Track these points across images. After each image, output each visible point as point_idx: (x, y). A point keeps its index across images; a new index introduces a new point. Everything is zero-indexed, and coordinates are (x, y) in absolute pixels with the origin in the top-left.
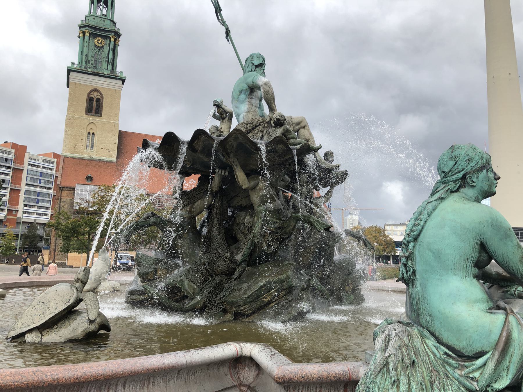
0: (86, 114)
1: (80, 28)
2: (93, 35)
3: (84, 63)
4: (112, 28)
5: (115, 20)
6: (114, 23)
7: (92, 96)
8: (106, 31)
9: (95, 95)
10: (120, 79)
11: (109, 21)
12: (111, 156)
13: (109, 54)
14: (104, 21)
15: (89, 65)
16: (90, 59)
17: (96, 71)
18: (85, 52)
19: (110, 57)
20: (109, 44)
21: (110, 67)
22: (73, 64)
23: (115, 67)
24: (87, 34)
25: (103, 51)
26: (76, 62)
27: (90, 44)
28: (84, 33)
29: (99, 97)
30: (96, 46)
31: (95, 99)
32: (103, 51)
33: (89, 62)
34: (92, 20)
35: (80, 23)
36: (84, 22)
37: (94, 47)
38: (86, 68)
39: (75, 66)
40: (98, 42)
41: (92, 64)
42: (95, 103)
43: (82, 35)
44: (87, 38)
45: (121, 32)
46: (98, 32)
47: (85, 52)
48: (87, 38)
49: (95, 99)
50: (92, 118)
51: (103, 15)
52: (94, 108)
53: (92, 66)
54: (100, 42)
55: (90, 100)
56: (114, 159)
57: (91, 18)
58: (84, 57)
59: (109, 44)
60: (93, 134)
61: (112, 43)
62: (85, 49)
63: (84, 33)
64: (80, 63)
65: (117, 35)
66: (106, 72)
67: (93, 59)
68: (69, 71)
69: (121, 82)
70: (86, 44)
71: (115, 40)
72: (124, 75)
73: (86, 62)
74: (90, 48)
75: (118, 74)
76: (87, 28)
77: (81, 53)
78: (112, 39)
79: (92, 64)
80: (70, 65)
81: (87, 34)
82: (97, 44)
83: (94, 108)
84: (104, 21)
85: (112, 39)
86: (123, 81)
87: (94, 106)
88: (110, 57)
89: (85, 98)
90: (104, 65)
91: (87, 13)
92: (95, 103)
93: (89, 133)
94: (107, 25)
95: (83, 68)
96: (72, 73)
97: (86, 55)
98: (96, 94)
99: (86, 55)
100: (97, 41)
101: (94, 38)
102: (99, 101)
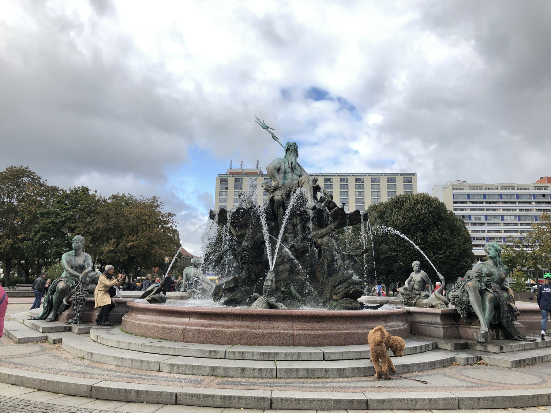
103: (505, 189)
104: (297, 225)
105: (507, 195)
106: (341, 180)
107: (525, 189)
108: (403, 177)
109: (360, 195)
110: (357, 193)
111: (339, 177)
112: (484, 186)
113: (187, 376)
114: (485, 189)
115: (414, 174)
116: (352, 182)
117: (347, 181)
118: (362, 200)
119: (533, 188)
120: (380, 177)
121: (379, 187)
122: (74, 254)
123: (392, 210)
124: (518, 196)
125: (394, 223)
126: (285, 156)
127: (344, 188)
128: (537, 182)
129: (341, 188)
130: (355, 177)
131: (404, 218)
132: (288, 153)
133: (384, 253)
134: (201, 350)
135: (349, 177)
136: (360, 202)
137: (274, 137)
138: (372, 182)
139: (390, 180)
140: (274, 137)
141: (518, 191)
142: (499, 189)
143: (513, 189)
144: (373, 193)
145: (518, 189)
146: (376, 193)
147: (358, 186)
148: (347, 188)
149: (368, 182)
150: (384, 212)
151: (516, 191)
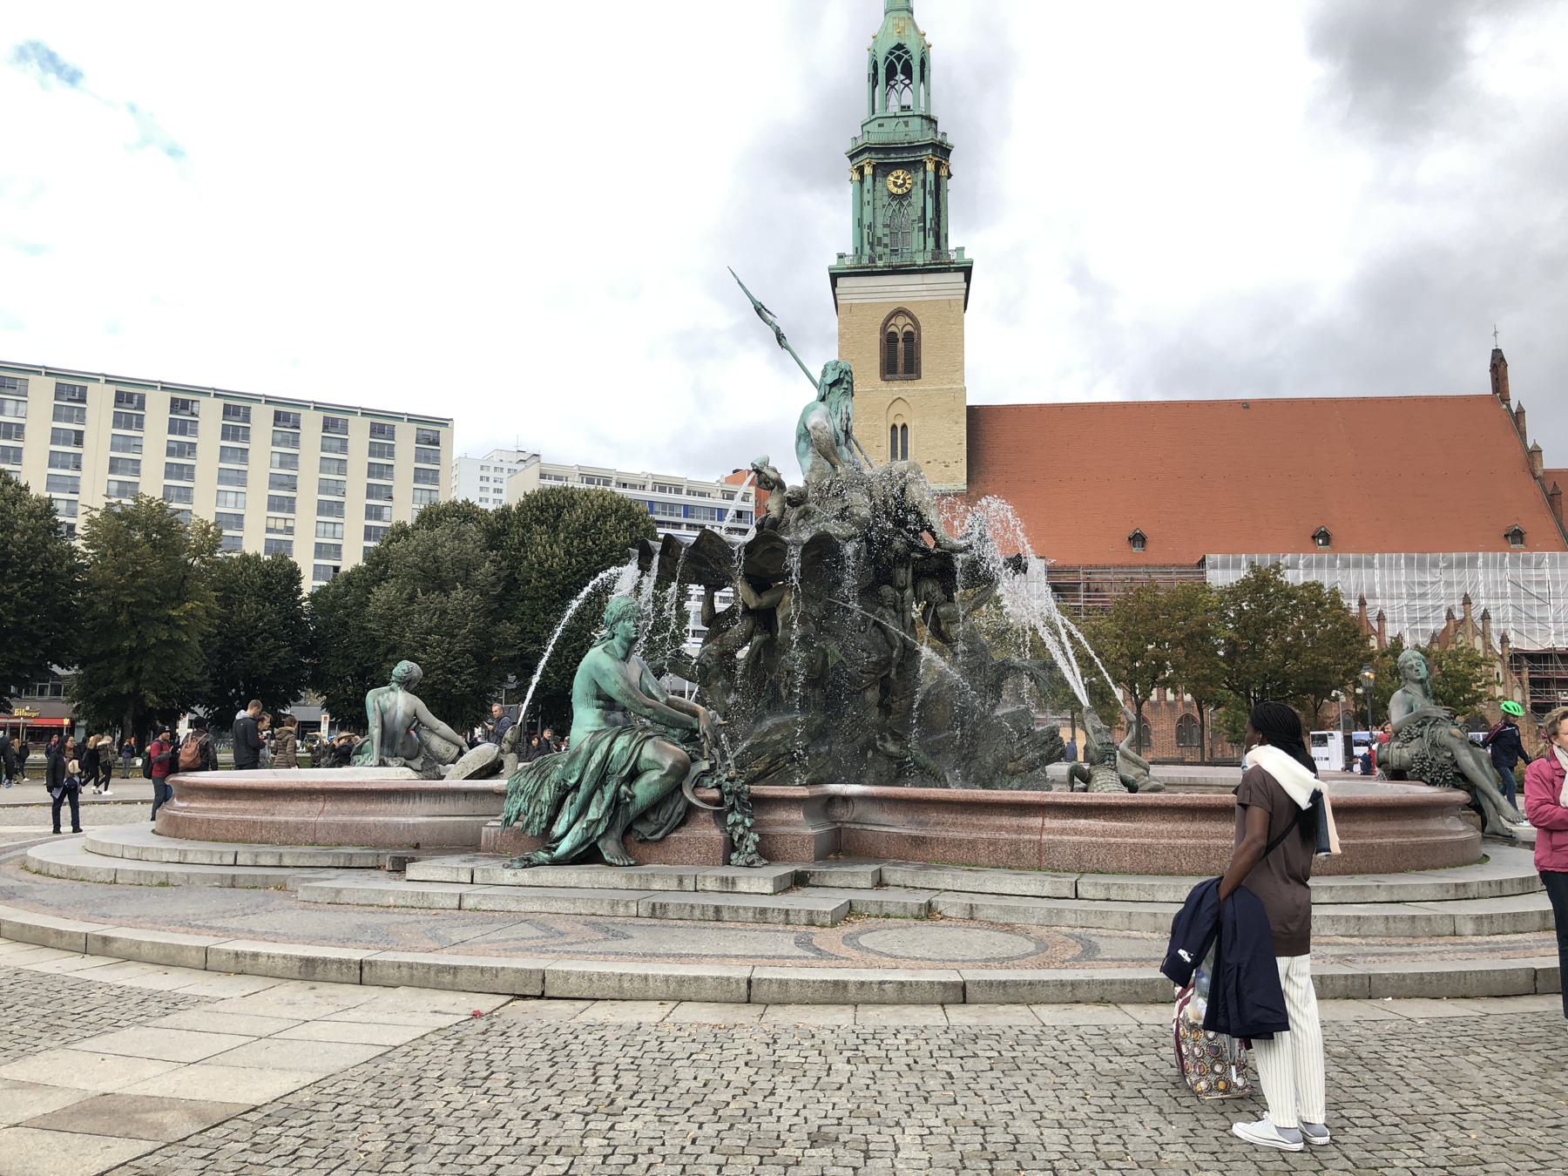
0: (883, 379)
1: (851, 158)
2: (882, 169)
3: (867, 248)
4: (929, 137)
5: (933, 114)
6: (931, 121)
7: (893, 329)
8: (912, 148)
9: (900, 326)
10: (958, 270)
11: (918, 121)
12: (953, 479)
13: (924, 209)
14: (906, 124)
15: (879, 249)
16: (879, 233)
17: (896, 261)
18: (866, 222)
19: (929, 214)
20: (924, 182)
21: (931, 242)
22: (841, 256)
23: (942, 240)
24: (868, 171)
25: (910, 204)
26: (850, 251)
27: (878, 195)
28: (861, 170)
29: (909, 328)
30: (893, 196)
31: (900, 336)
32: (910, 204)
33: (880, 239)
34: (877, 129)
35: (849, 147)
36: (860, 142)
37: (886, 200)
38: (872, 260)
39: (847, 262)
40: (895, 184)
41: (886, 246)
42: (901, 345)
43: (856, 177)
44: (869, 180)
45: (949, 140)
46: (894, 158)
47: (866, 222)
48: (869, 180)
49: (900, 336)
50: (898, 388)
51: (903, 108)
52: (901, 361)
53: (887, 251)
54: (900, 182)
55: (889, 340)
56: (962, 485)
57: (873, 127)
58: (866, 231)
59: (924, 182)
60: (904, 427)
61: (931, 177)
62: (868, 210)
63: (861, 170)
64: (859, 251)
65: (942, 151)
66: (920, 262)
67: (887, 231)
68: (834, 277)
69: (961, 276)
70: (867, 197)
71: (938, 166)
72: (967, 256)
73: (871, 245)
74: (879, 204)
75: (953, 257)
76: (866, 155)
77: (860, 223)
78: (930, 167)
79: (886, 246)
80: (834, 262)
81: (868, 171)
82: (895, 190)
83: (901, 361)
84: (906, 124)
85: (930, 167)
86: (967, 271)
87: (901, 354)
88: (929, 214)
89: (877, 336)
90: (916, 239)
91: (865, 115)
92: (901, 345)
93: (894, 427)
94: (915, 132)
95: (865, 261)
96: (840, 280)
97: (869, 227)
98: (901, 321)
99: (869, 227)
100: (895, 181)
101: (885, 176)
102: (912, 339)
103: (662, 489)
104: (905, 588)
105: (664, 505)
106: (228, 411)
107: (702, 494)
108: (415, 425)
109: (282, 465)
110: (277, 458)
111: (168, 395)
112: (615, 478)
113: (1508, 937)
114: (618, 484)
115: (444, 423)
116: (262, 420)
117: (247, 418)
118: (286, 481)
119: (719, 494)
120: (350, 418)
121: (344, 447)
122: (620, 653)
123: (528, 528)
124: (688, 510)
125: (540, 564)
126: (823, 399)
127: (235, 438)
128: (728, 480)
129: (224, 436)
130: (272, 408)
131: (568, 553)
132: (837, 391)
133: (506, 646)
134: (1441, 885)
135: (149, 393)
136: (281, 486)
137: (780, 338)
138: (325, 428)
139: (376, 430)
140: (780, 338)
141: (691, 498)
142: (649, 487)
143: (678, 491)
144: (326, 463)
145: (689, 493)
146: (336, 464)
147: (279, 436)
148: (246, 437)
149: (311, 427)
150: (503, 532)
151: (684, 498)
